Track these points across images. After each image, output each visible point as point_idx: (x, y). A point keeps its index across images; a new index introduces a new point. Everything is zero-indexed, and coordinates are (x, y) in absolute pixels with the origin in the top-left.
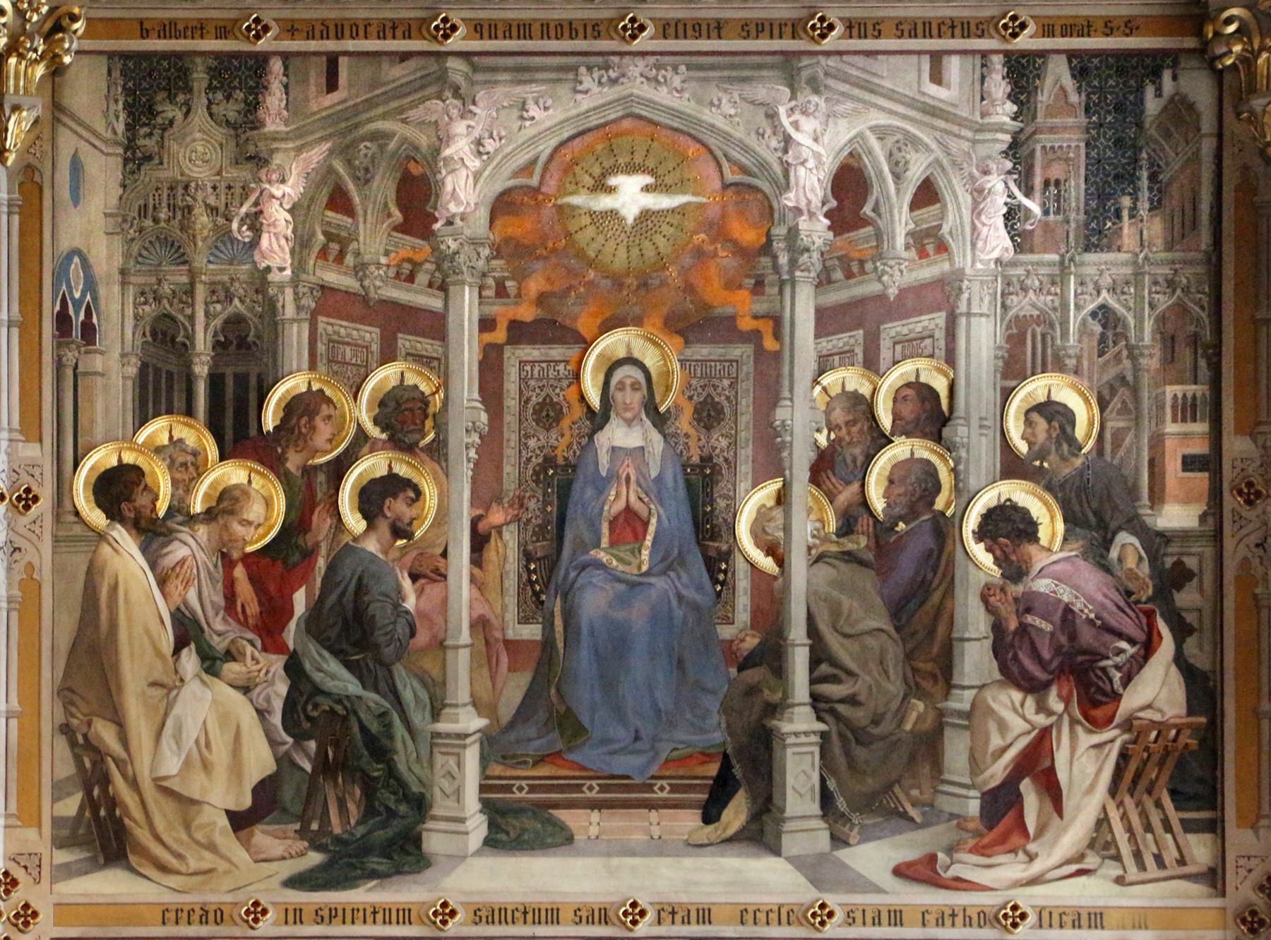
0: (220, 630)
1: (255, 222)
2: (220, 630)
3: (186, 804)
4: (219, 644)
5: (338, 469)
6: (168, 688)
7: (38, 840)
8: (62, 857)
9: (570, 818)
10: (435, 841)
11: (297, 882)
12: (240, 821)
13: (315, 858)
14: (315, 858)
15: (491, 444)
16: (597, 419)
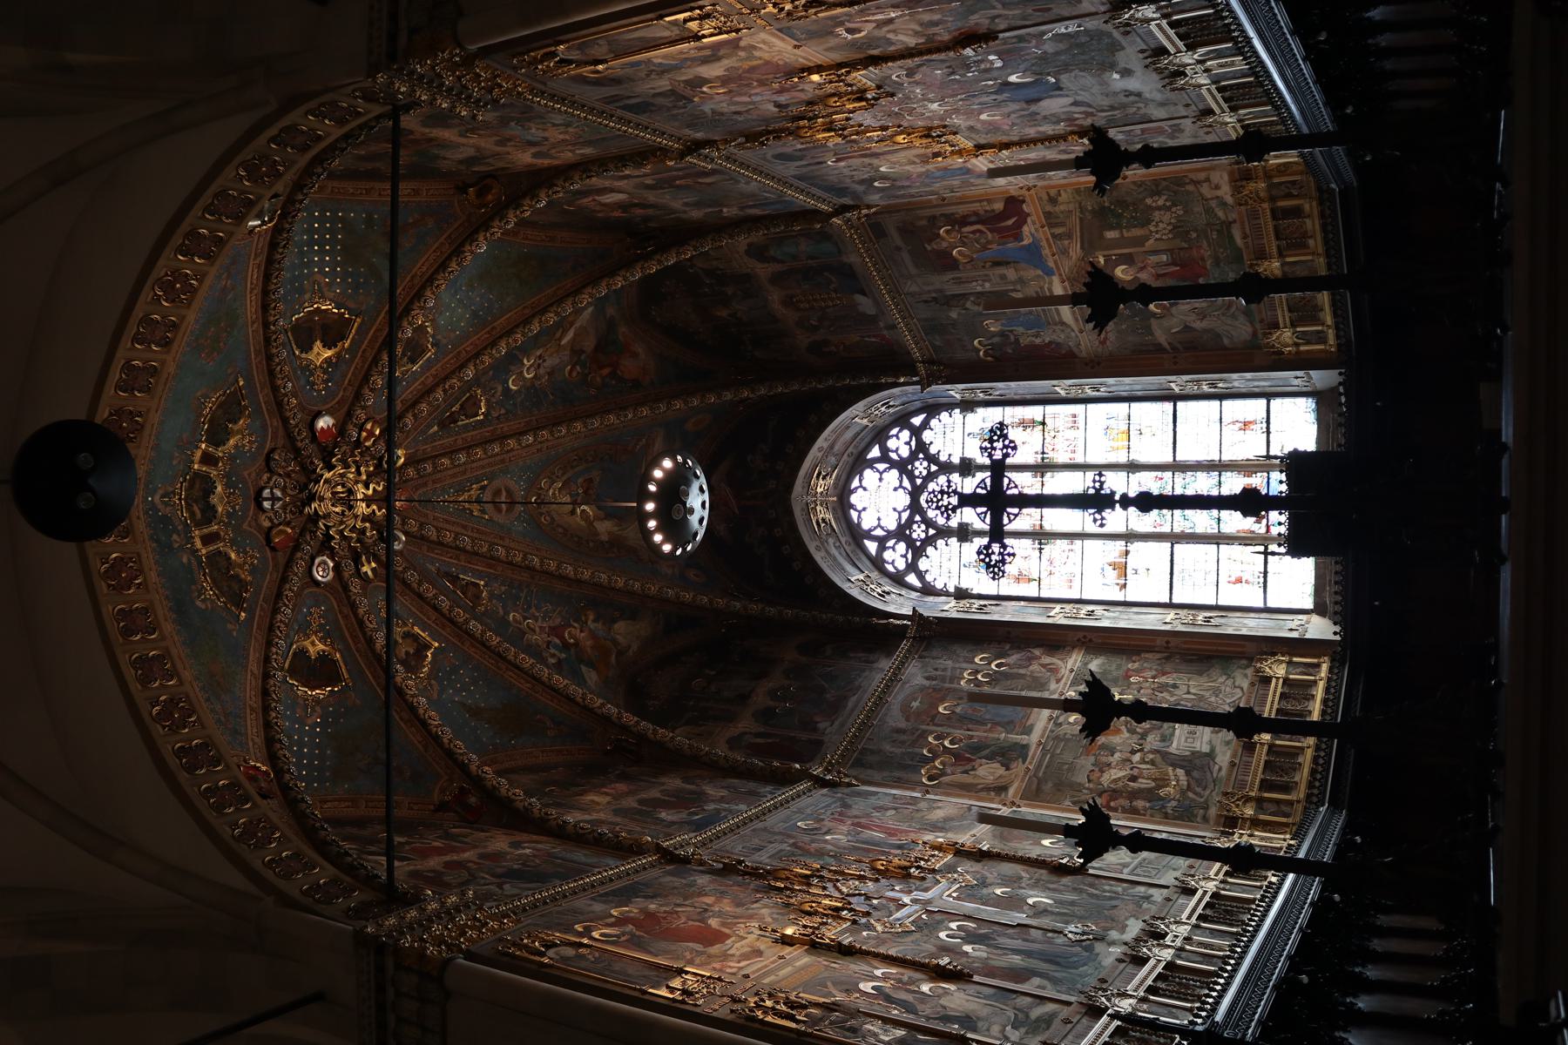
0: (968, 767)
1: (891, 753)
2: (967, 767)
3: (1000, 776)
4: (970, 768)
5: (944, 747)
6: (975, 776)
7: (998, 799)
8: (1003, 795)
9: (1029, 723)
10: (1025, 743)
11: (1024, 763)
12: (1008, 769)
13: (1020, 760)
14: (1020, 760)
15: (950, 726)
16: (953, 712)
